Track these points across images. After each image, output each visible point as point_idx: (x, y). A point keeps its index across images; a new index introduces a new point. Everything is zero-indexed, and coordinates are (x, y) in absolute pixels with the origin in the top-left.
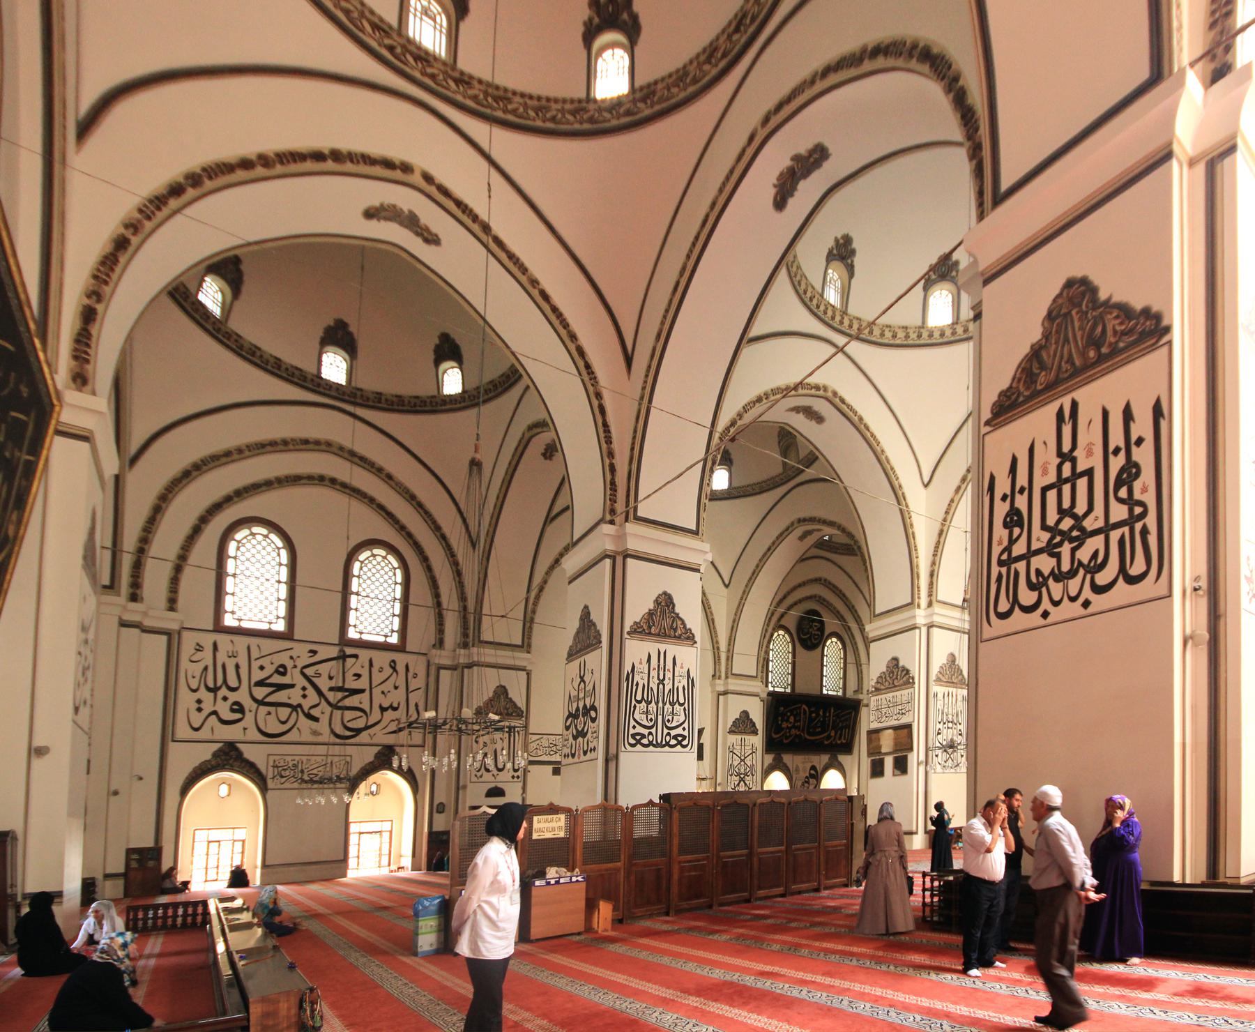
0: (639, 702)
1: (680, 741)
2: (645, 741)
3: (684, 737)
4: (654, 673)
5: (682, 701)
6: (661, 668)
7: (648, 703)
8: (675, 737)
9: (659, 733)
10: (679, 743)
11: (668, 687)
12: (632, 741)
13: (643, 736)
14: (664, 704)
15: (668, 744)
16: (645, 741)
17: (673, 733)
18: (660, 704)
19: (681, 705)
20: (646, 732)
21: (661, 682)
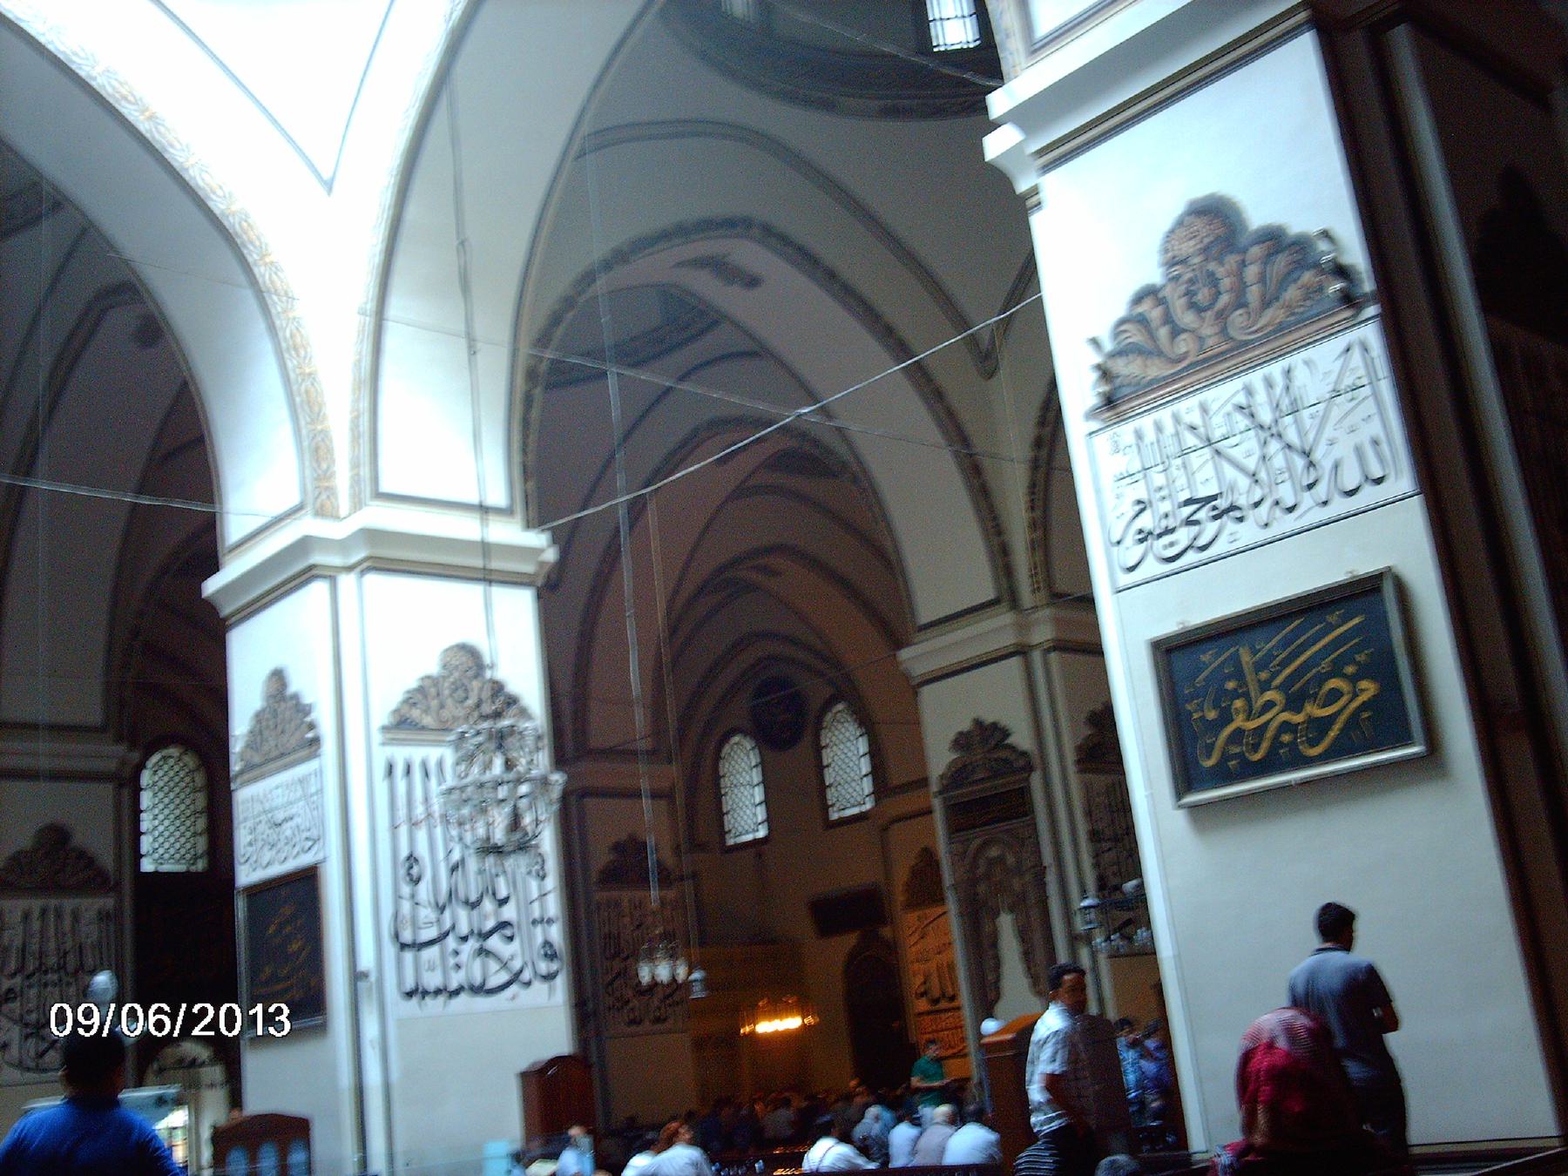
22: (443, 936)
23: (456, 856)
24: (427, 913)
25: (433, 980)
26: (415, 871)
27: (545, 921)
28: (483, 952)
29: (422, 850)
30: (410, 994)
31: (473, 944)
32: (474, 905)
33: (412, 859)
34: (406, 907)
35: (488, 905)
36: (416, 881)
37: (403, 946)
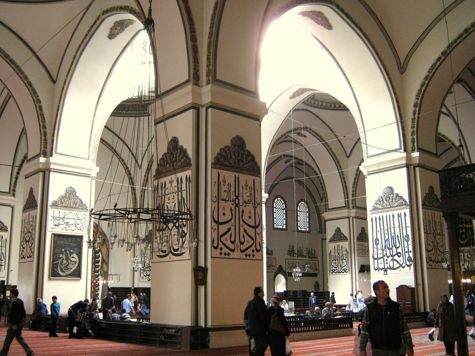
1: (345, 271)
2: (335, 272)
3: (346, 269)
4: (336, 252)
6: (338, 250)
7: (335, 260)
8: (344, 270)
9: (339, 269)
10: (345, 271)
11: (341, 255)
13: (335, 270)
16: (335, 272)
17: (343, 268)
20: (335, 269)
21: (339, 254)
22: (384, 256)
23: (387, 237)
24: (380, 251)
25: (381, 266)
26: (378, 242)
27: (409, 252)
28: (393, 260)
29: (379, 237)
30: (376, 270)
31: (391, 258)
32: (390, 249)
33: (377, 239)
34: (375, 250)
35: (394, 249)
36: (377, 244)
37: (375, 259)
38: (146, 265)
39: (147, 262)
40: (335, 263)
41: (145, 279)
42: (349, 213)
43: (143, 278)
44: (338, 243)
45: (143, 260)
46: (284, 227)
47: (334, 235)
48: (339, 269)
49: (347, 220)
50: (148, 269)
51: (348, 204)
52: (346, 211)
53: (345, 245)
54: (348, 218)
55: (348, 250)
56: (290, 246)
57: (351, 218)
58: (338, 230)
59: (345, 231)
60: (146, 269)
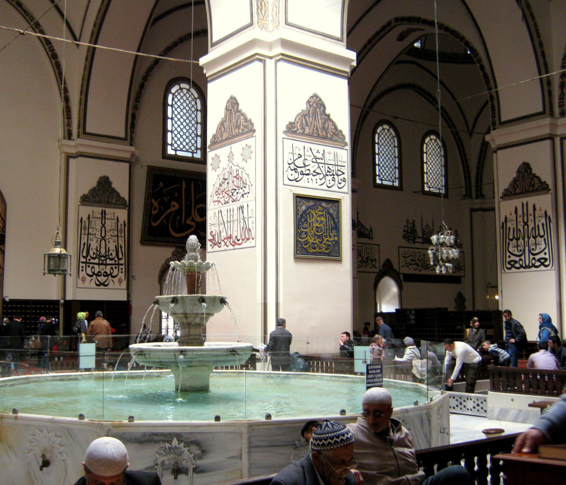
0: (511, 240)
1: (543, 262)
2: (517, 265)
3: (546, 260)
4: (520, 219)
5: (542, 233)
7: (518, 239)
8: (539, 260)
10: (542, 264)
12: (509, 266)
13: (516, 262)
14: (529, 238)
15: (534, 266)
17: (537, 257)
18: (526, 239)
19: (541, 237)
20: (517, 259)
38: (91, 253)
39: (94, 245)
40: (518, 246)
41: (91, 283)
42: (553, 126)
43: (84, 280)
44: (525, 200)
45: (84, 240)
46: (396, 184)
47: (515, 180)
48: (527, 259)
49: (548, 143)
50: (96, 261)
51: (551, 108)
52: (547, 121)
53: (543, 202)
54: (551, 138)
55: (550, 213)
56: (407, 221)
57: (558, 141)
58: (525, 168)
59: (543, 170)
60: (92, 261)
